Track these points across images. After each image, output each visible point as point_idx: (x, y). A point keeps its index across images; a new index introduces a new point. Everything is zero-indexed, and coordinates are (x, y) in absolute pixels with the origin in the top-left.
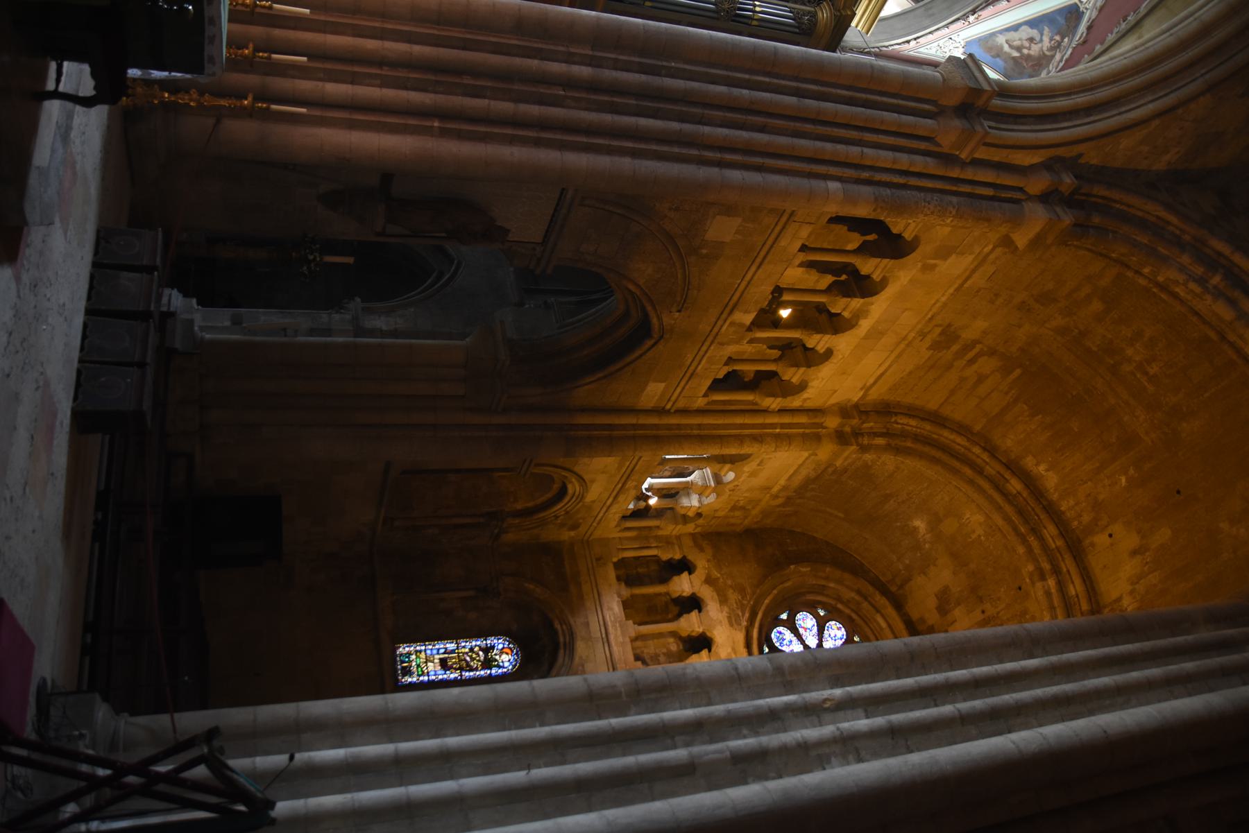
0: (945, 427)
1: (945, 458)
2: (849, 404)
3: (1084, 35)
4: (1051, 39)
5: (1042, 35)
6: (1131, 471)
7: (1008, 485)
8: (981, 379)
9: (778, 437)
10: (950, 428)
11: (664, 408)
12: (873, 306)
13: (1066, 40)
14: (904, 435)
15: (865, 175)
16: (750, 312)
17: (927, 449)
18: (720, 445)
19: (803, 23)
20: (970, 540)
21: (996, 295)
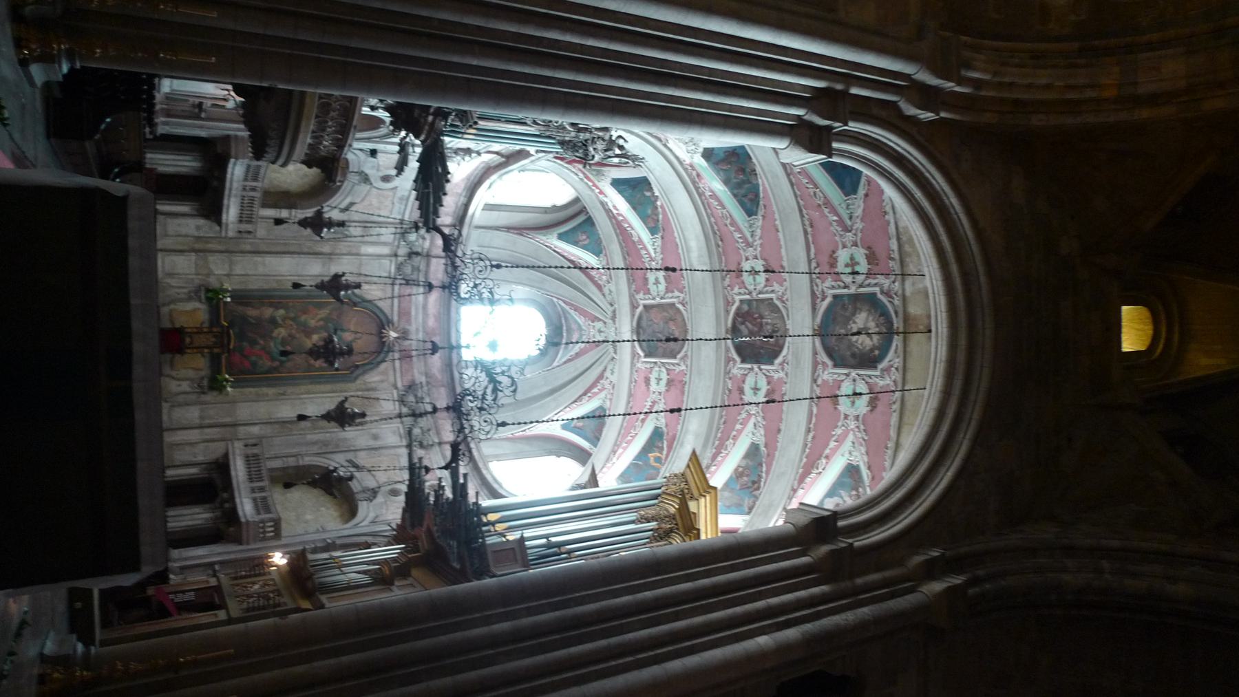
3: (869, 474)
4: (850, 496)
5: (842, 498)
13: (860, 490)
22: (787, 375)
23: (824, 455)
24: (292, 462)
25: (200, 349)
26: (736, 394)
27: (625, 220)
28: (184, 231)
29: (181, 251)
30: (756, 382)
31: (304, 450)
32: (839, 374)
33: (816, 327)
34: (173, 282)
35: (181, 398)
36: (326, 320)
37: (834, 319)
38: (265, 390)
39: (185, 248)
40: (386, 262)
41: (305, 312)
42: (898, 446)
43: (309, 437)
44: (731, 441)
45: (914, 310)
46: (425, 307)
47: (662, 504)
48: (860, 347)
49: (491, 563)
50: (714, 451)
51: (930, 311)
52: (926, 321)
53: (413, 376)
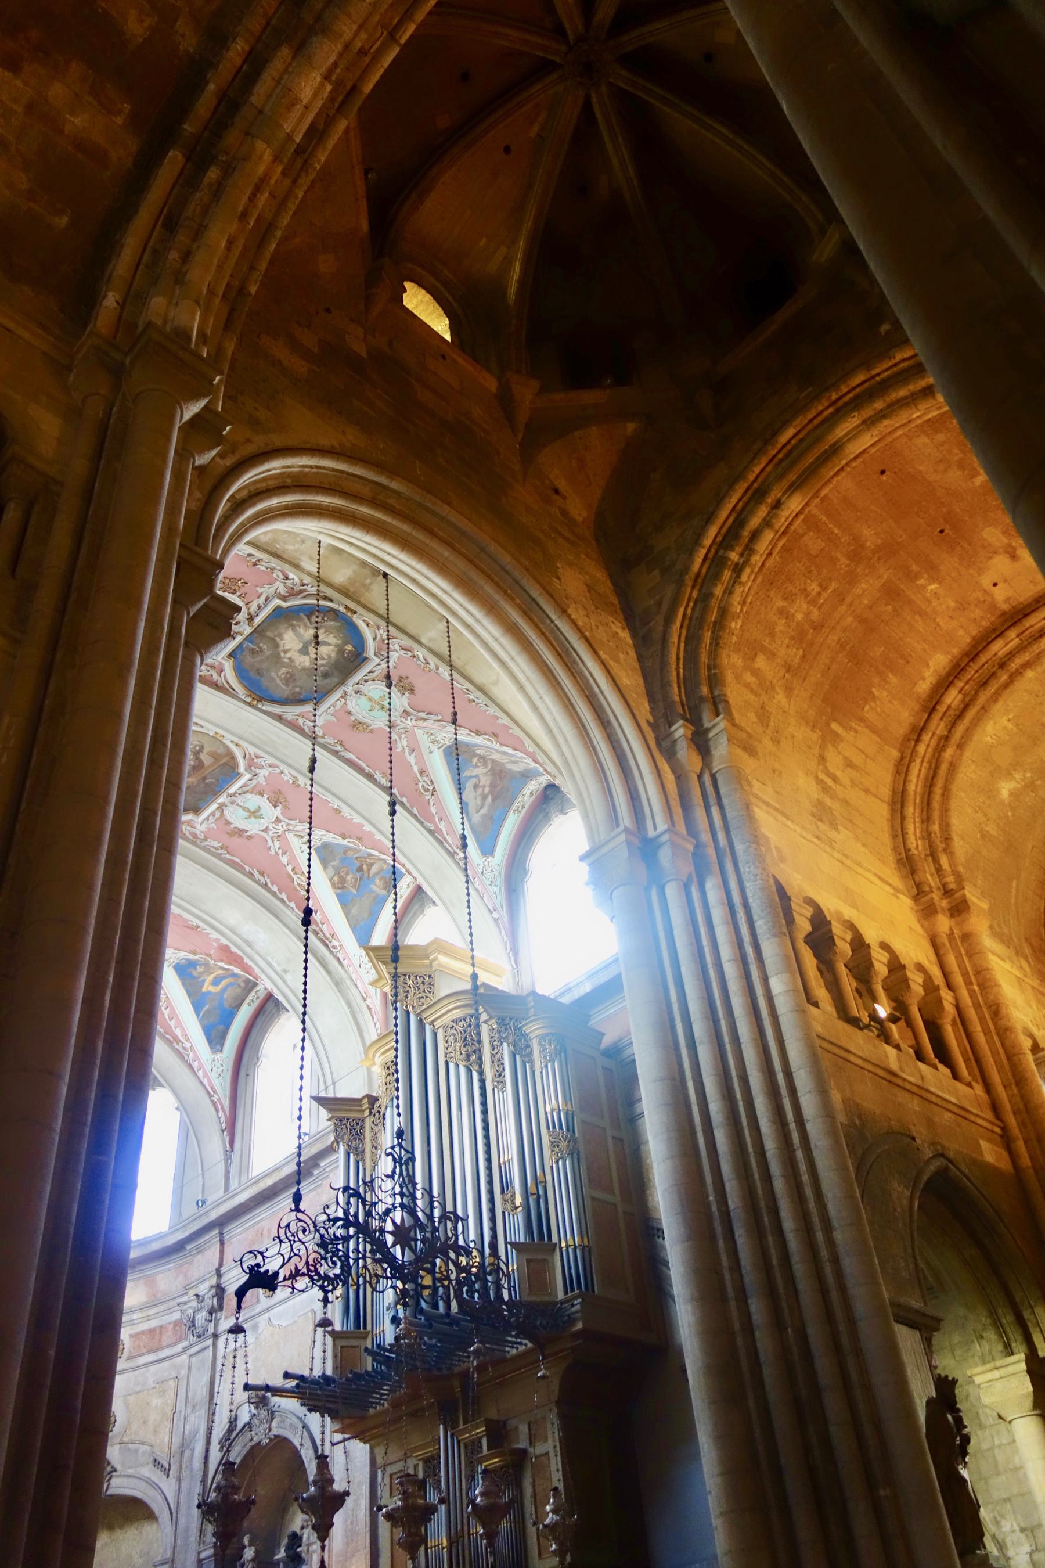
0: (904, 791)
1: (940, 783)
2: (915, 908)
3: (487, 737)
4: (476, 766)
5: (471, 777)
6: (921, 582)
7: (953, 706)
8: (849, 764)
9: (982, 986)
10: (904, 784)
11: (1002, 1136)
12: (830, 908)
13: (478, 752)
14: (928, 836)
15: (750, 951)
16: (885, 1052)
17: (936, 804)
18: (1021, 1056)
19: (555, 1049)
20: (1015, 729)
21: (774, 771)
22: (270, 766)
23: (418, 775)
26: (235, 842)
30: (244, 809)
32: (334, 705)
33: (249, 700)
37: (259, 672)
42: (481, 689)
44: (294, 877)
45: (341, 575)
47: (437, 1024)
48: (324, 662)
49: (547, 1299)
50: (293, 905)
51: (358, 559)
52: (367, 571)
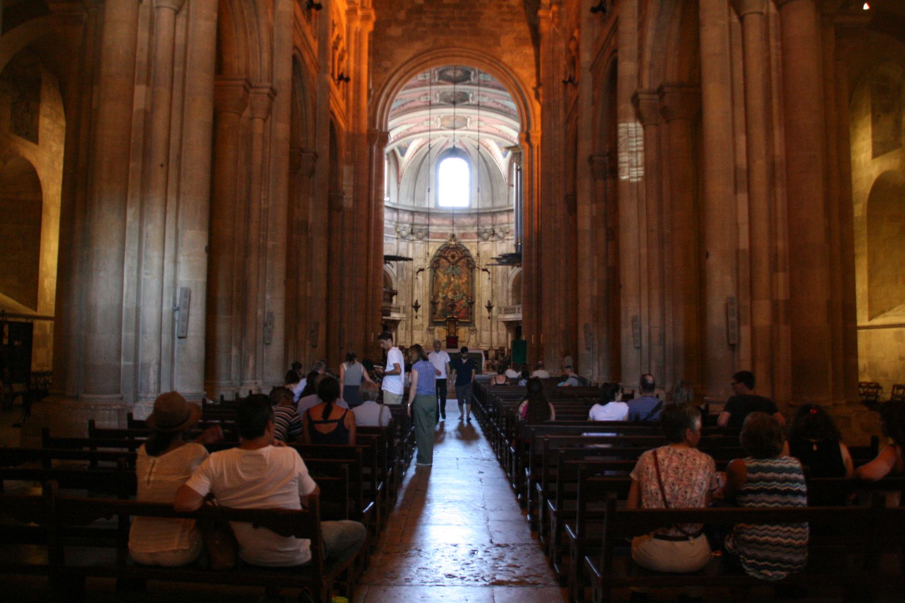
24: (510, 294)
25: (456, 330)
27: (397, 135)
28: (404, 335)
29: (412, 336)
31: (505, 289)
34: (425, 340)
35: (478, 339)
36: (444, 274)
38: (476, 303)
39: (410, 334)
40: (417, 245)
41: (440, 284)
43: (500, 284)
46: (439, 225)
53: (473, 233)
